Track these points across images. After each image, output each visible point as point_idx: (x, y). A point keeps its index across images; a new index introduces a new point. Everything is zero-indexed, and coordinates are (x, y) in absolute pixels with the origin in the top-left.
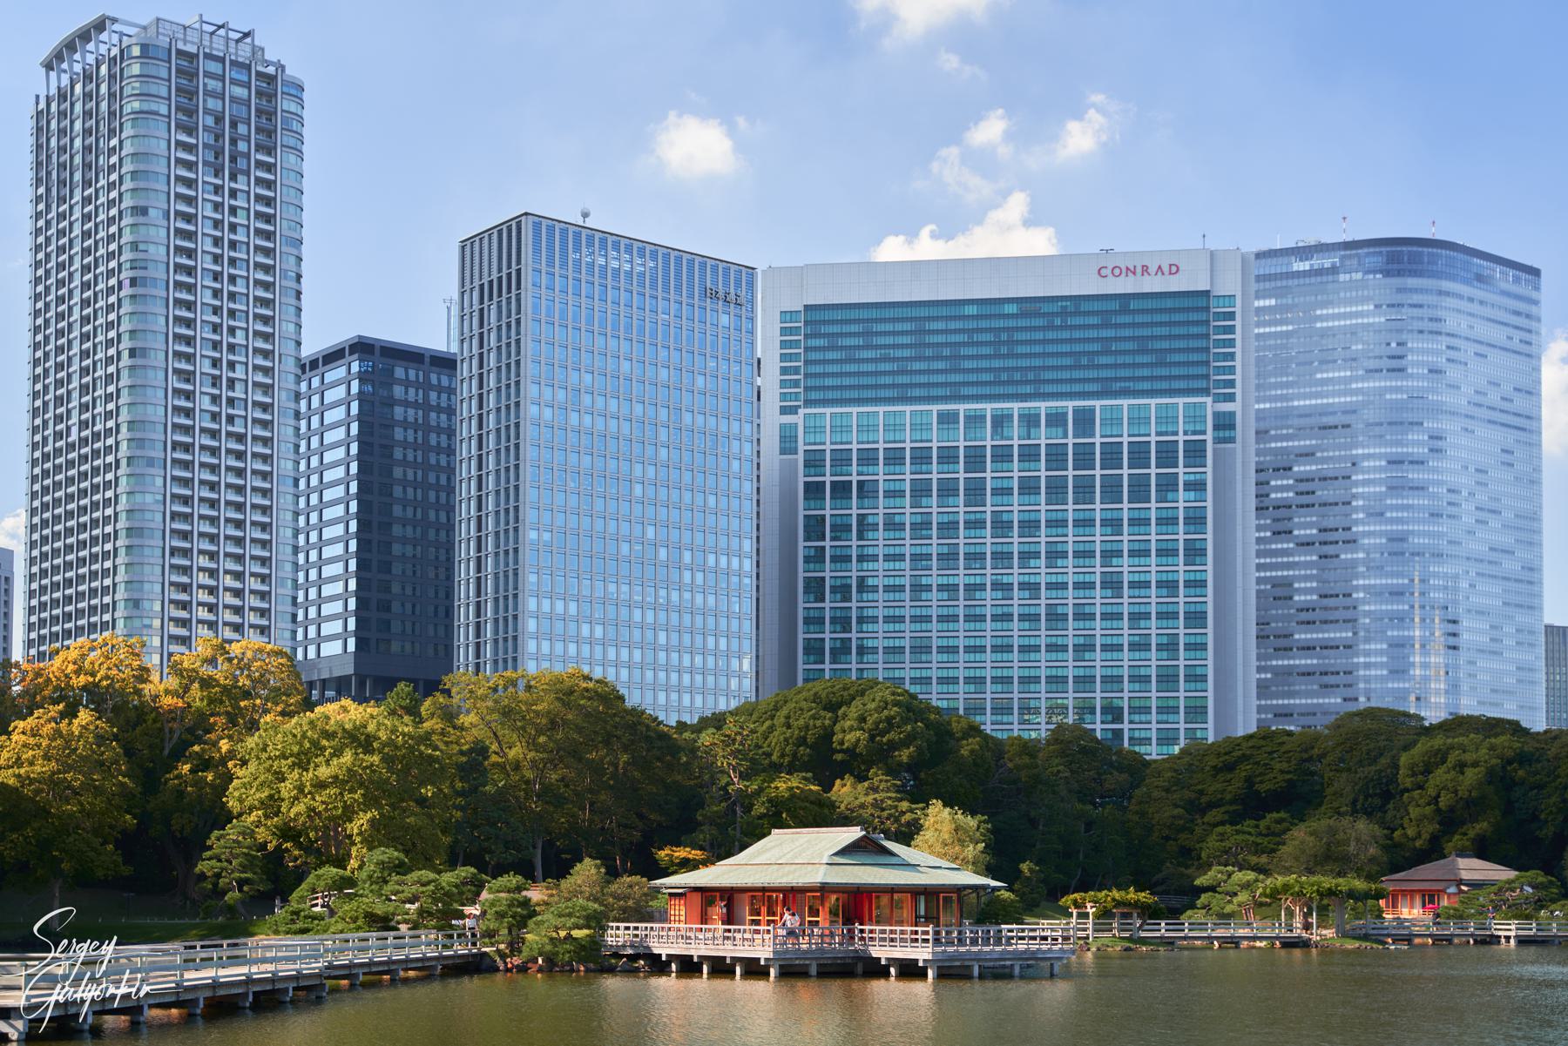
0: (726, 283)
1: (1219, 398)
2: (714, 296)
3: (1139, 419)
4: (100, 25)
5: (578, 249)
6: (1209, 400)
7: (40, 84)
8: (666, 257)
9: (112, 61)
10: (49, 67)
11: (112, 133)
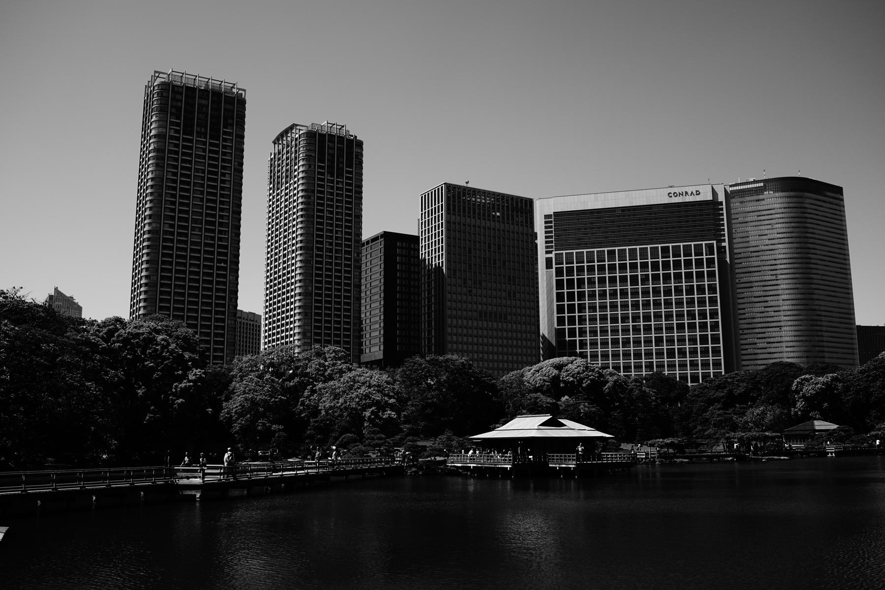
4: (291, 128)
6: (715, 242)
7: (271, 149)
9: (296, 139)
10: (274, 143)
11: (295, 164)
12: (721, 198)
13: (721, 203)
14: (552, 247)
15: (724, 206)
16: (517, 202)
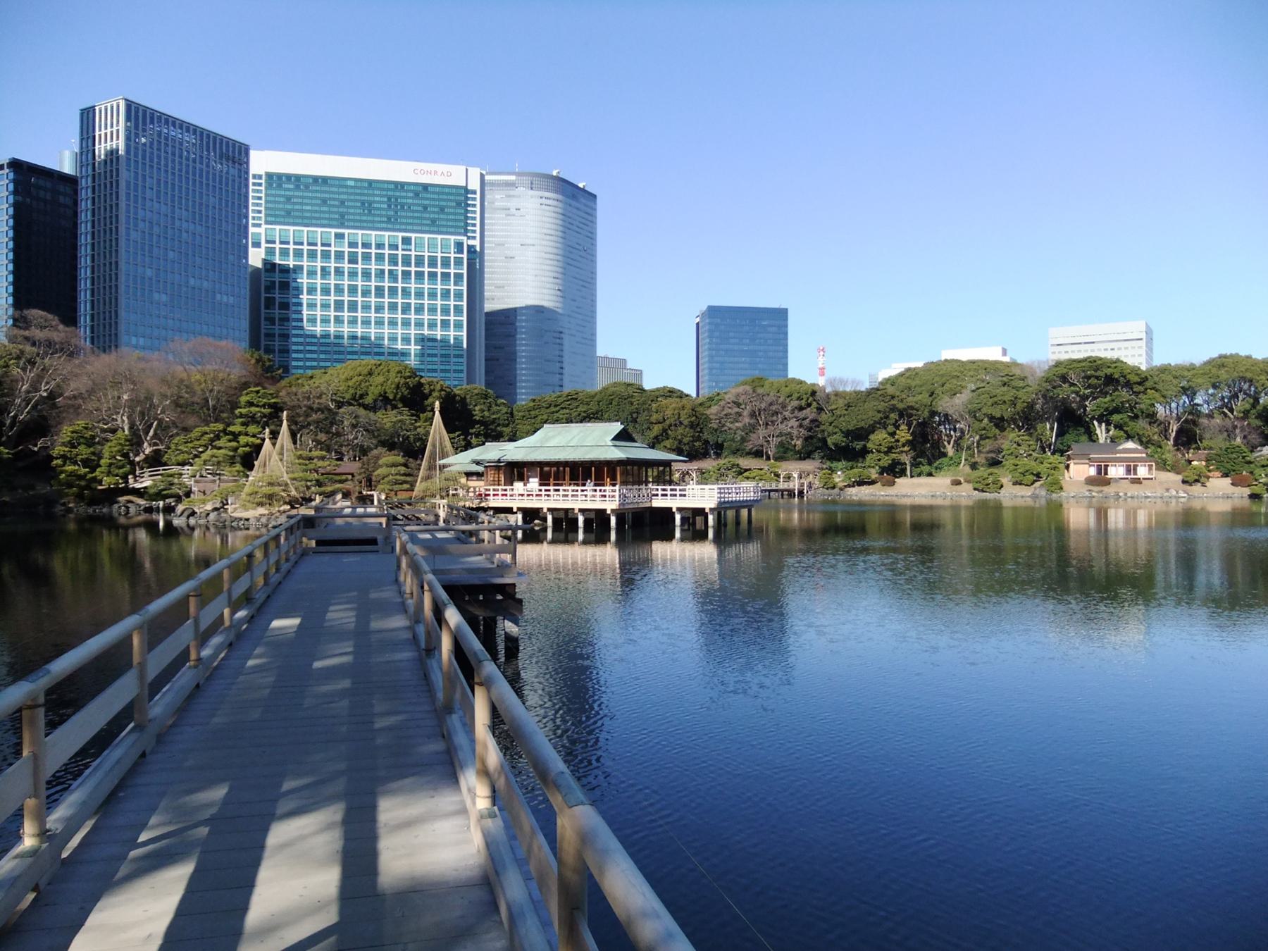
0: (234, 152)
1: (469, 238)
2: (228, 159)
3: (432, 245)
5: (152, 122)
8: (202, 134)
12: (474, 185)
13: (474, 192)
14: (260, 218)
15: (478, 196)
16: (227, 143)
